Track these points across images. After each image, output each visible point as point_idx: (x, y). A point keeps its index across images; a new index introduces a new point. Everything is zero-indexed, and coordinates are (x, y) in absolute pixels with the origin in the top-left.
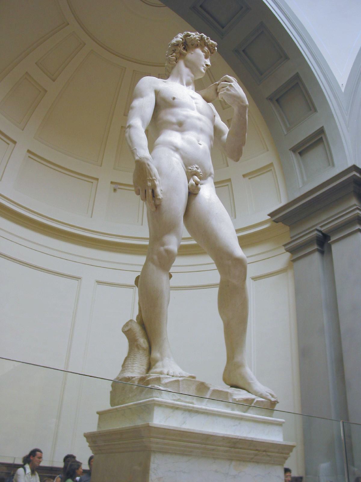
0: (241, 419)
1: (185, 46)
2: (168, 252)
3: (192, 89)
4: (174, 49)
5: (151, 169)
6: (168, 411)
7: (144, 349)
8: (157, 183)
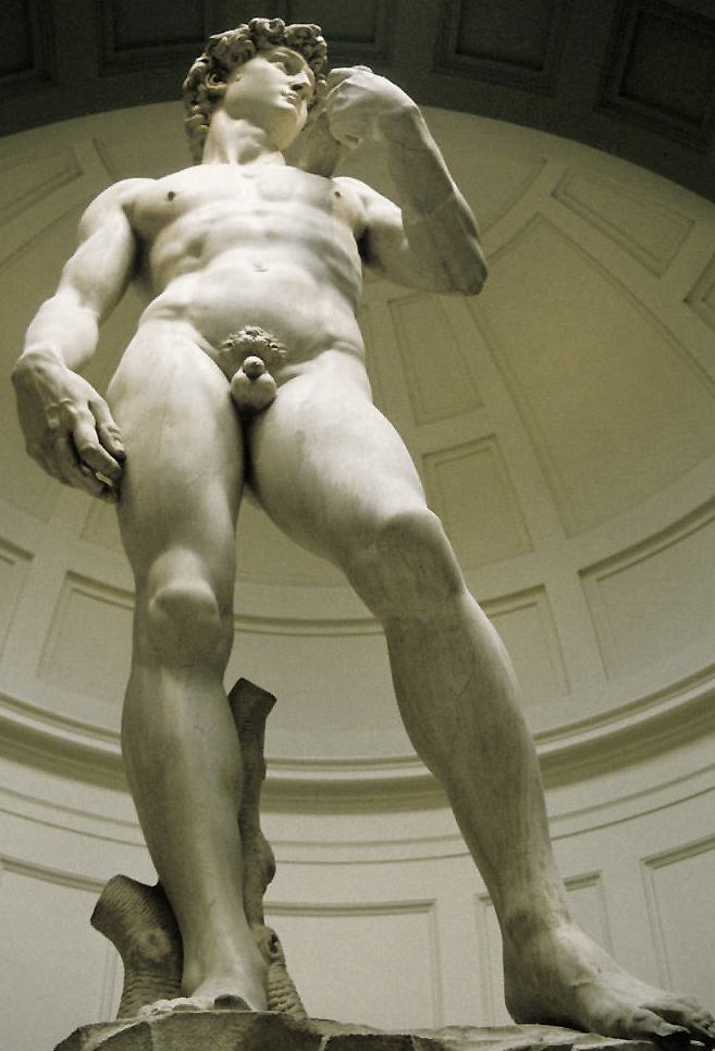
4: (193, 99)
5: (49, 379)
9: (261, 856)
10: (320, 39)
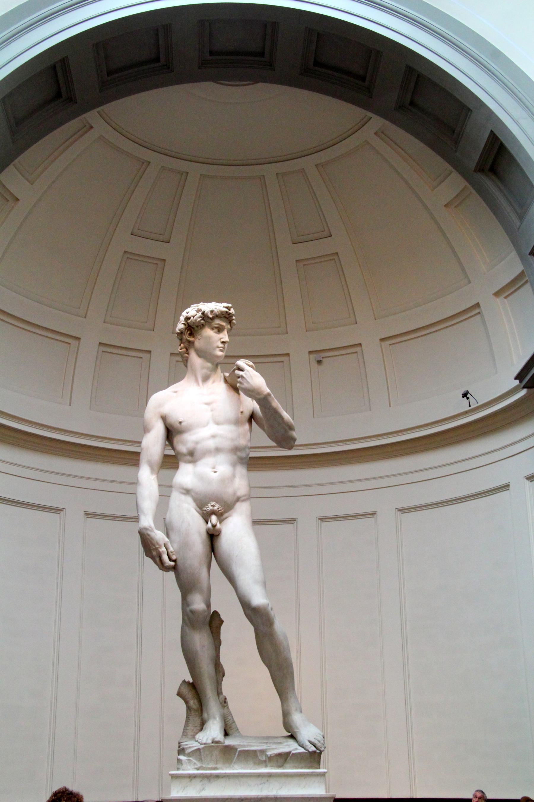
0: (270, 775)
1: (191, 331)
2: (192, 612)
3: (214, 382)
5: (152, 538)
6: (185, 781)
7: (195, 710)
8: (163, 549)
9: (221, 673)
10: (232, 311)
